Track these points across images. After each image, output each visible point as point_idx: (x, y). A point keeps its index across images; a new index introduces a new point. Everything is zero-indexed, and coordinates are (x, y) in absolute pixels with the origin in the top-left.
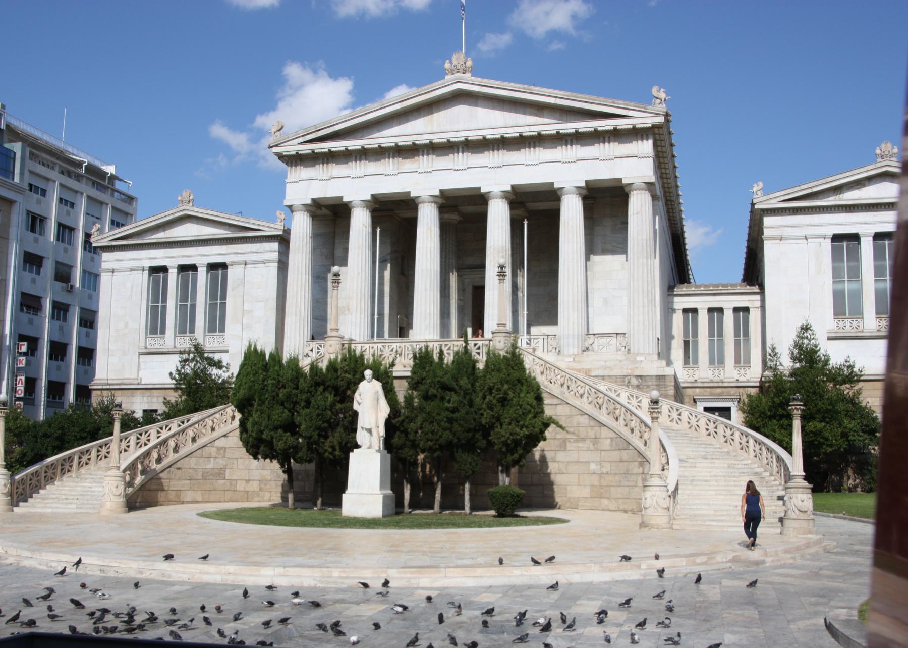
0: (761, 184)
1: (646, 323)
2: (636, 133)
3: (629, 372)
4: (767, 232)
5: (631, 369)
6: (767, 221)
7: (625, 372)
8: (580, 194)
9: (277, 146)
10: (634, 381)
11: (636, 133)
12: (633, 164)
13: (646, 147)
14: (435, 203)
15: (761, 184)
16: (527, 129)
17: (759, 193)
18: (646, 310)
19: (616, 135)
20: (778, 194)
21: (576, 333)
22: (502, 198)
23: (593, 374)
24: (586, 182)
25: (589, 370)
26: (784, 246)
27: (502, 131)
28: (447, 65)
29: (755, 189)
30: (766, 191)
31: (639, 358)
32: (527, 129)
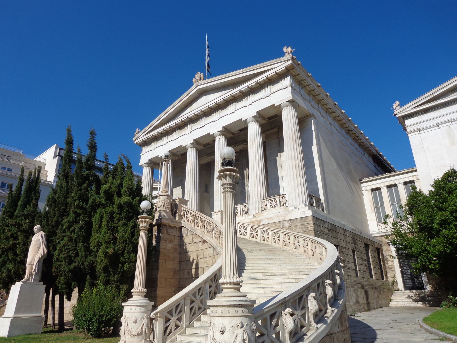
0: (397, 103)
1: (296, 184)
2: (279, 77)
3: (283, 218)
4: (408, 129)
5: (284, 217)
6: (408, 122)
7: (281, 219)
8: (257, 121)
9: (136, 140)
10: (287, 224)
11: (279, 77)
12: (280, 94)
13: (287, 81)
14: (194, 147)
15: (397, 103)
16: (226, 95)
17: (398, 108)
18: (295, 176)
19: (271, 81)
20: (410, 104)
21: (257, 200)
22: (220, 135)
23: (262, 224)
24: (257, 112)
25: (260, 221)
26: (424, 134)
27: (215, 101)
28: (194, 80)
29: (394, 107)
30: (401, 105)
31: (290, 209)
32: (226, 95)
